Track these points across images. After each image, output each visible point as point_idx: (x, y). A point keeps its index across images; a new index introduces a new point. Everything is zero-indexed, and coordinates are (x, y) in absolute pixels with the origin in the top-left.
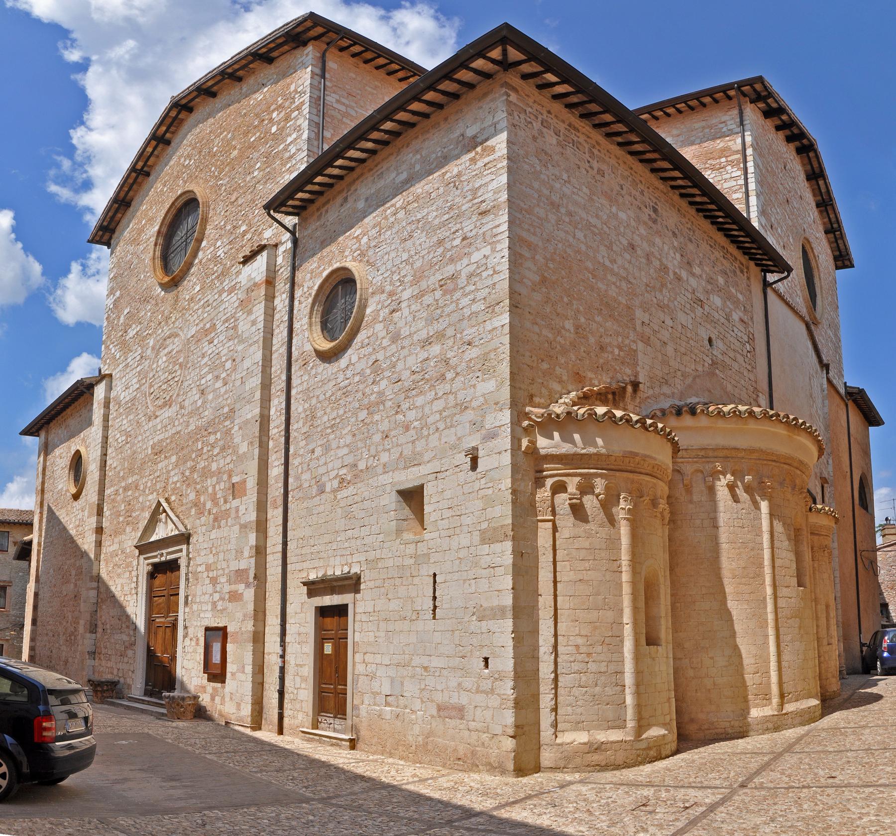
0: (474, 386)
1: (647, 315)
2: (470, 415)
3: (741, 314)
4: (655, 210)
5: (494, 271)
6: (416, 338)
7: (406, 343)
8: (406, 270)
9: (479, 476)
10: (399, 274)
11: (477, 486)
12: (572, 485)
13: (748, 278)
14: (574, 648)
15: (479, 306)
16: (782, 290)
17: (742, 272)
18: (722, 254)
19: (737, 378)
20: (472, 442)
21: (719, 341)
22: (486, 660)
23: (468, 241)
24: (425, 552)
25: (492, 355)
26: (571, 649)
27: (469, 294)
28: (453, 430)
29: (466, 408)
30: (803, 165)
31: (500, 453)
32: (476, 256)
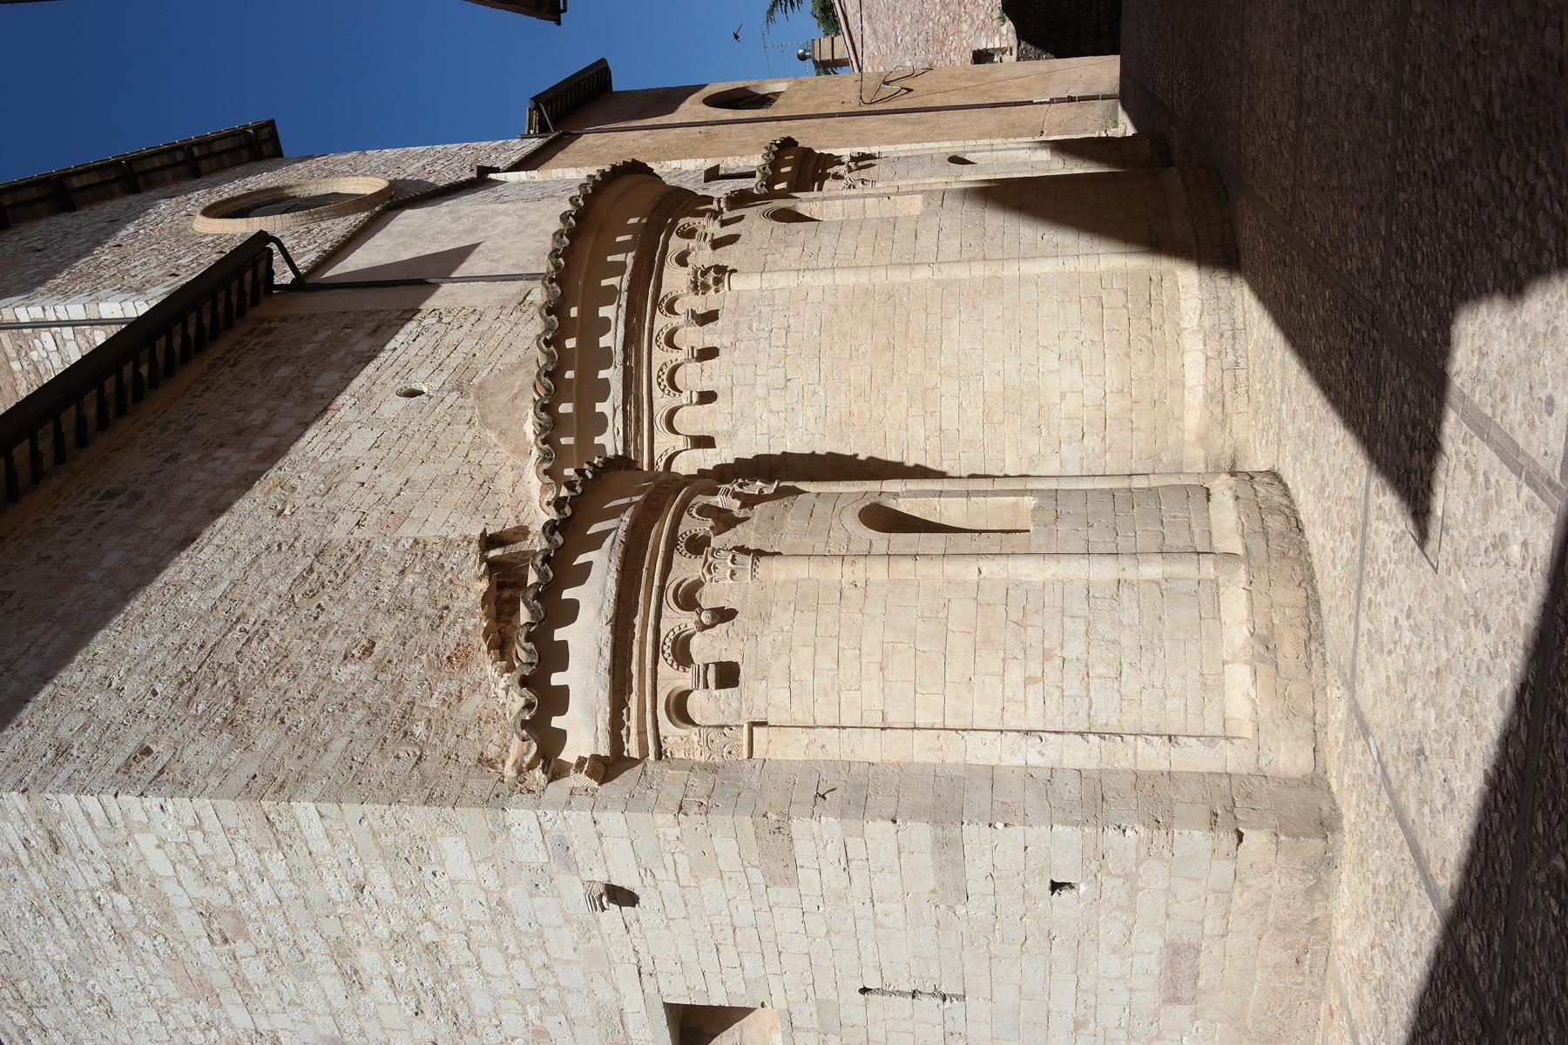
0: (453, 882)
1: (342, 517)
2: (516, 895)
3: (359, 334)
4: (111, 495)
5: (195, 828)
6: (340, 1003)
7: (351, 1025)
8: (182, 1013)
9: (649, 881)
10: (189, 1030)
11: (669, 887)
12: (673, 678)
13: (284, 319)
14: (1031, 689)
15: (276, 864)
16: (312, 256)
17: (269, 331)
18: (225, 369)
19: (492, 343)
20: (575, 894)
21: (413, 377)
22: (1055, 886)
23: (121, 880)
24: (814, 1009)
25: (388, 841)
26: (1034, 693)
27: (247, 885)
28: (548, 933)
29: (500, 902)
30: (36, 217)
31: (600, 836)
32: (160, 864)
